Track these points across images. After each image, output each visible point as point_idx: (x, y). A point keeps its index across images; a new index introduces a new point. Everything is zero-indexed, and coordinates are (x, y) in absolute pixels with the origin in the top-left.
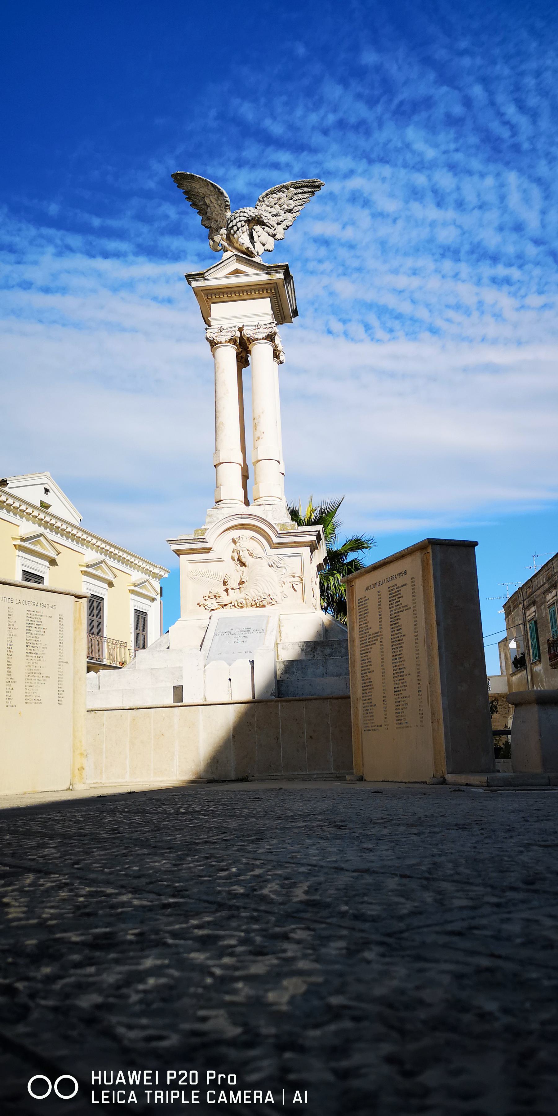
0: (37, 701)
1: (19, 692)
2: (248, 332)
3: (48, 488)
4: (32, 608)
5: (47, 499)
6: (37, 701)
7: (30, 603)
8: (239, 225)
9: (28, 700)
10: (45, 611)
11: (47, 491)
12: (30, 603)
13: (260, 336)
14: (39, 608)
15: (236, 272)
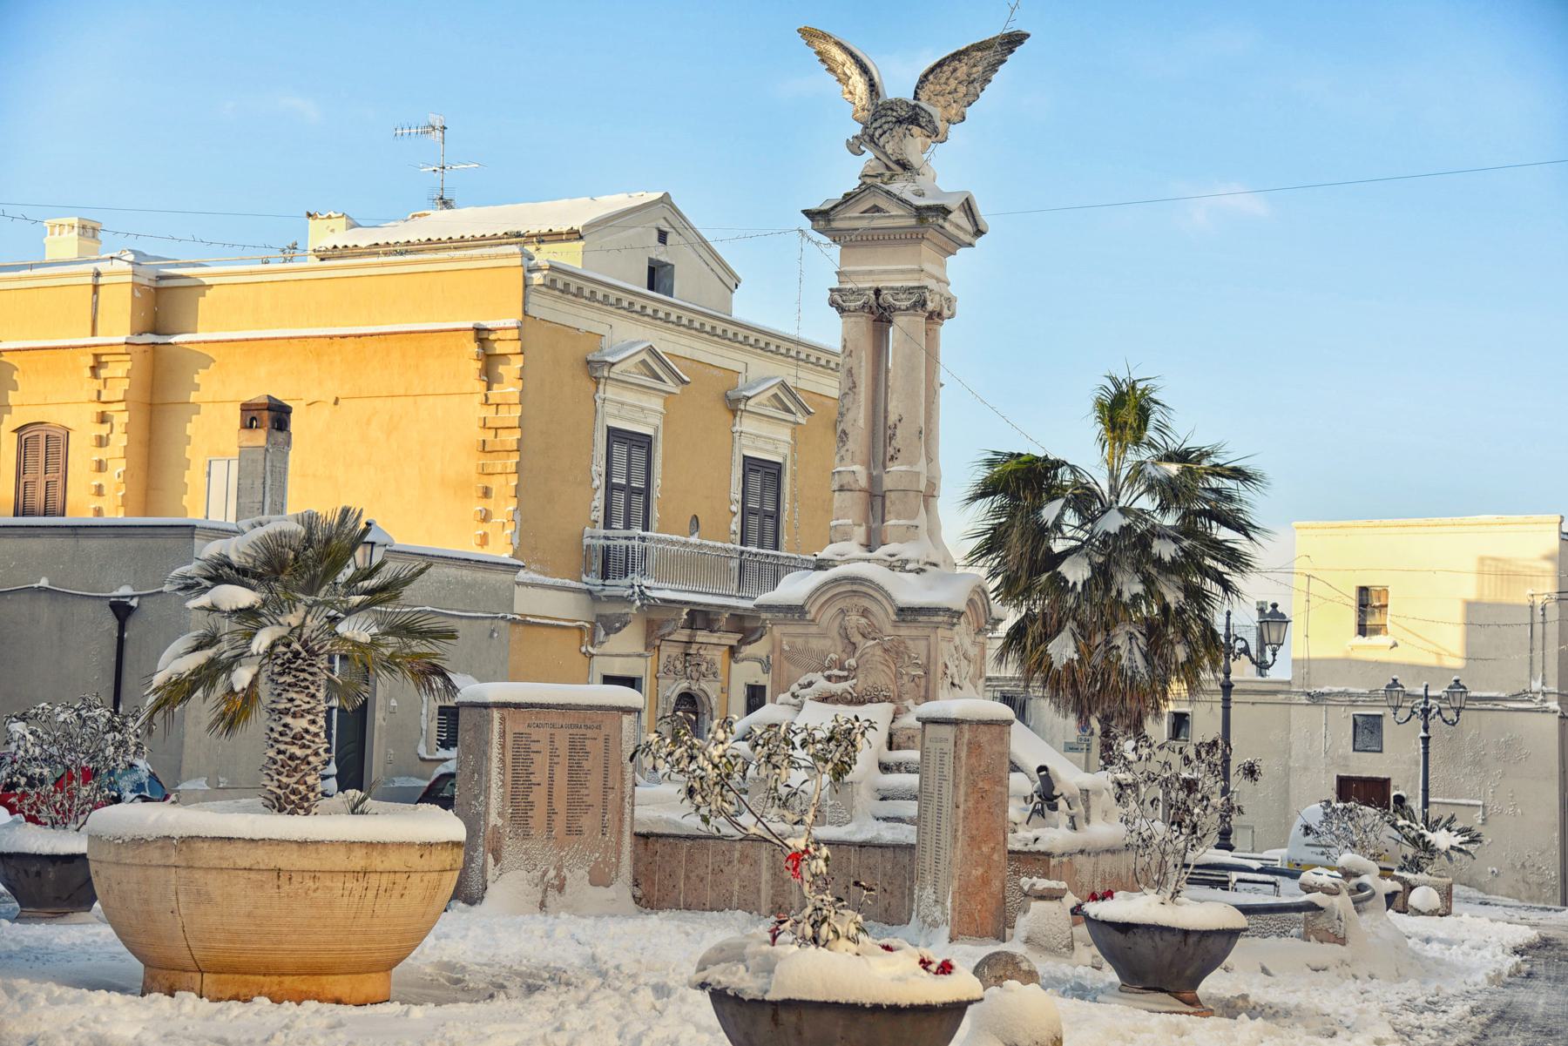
0: (580, 832)
1: (560, 823)
2: (887, 297)
3: (666, 228)
4: (575, 731)
5: (661, 254)
6: (580, 832)
7: (571, 726)
8: (886, 127)
9: (569, 831)
10: (590, 733)
11: (663, 236)
12: (571, 726)
13: (904, 304)
14: (583, 731)
15: (876, 209)
